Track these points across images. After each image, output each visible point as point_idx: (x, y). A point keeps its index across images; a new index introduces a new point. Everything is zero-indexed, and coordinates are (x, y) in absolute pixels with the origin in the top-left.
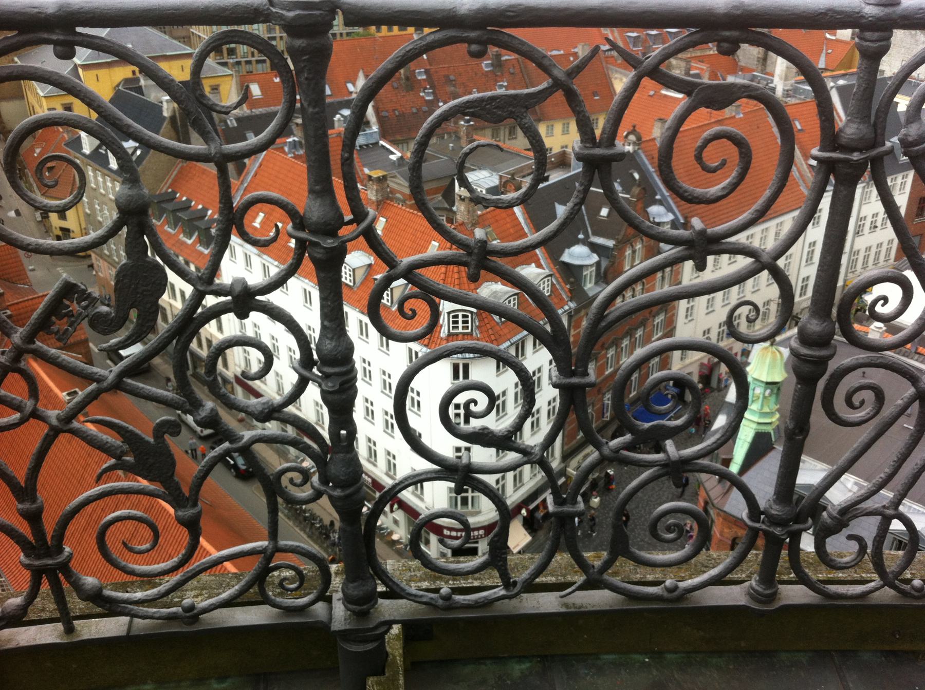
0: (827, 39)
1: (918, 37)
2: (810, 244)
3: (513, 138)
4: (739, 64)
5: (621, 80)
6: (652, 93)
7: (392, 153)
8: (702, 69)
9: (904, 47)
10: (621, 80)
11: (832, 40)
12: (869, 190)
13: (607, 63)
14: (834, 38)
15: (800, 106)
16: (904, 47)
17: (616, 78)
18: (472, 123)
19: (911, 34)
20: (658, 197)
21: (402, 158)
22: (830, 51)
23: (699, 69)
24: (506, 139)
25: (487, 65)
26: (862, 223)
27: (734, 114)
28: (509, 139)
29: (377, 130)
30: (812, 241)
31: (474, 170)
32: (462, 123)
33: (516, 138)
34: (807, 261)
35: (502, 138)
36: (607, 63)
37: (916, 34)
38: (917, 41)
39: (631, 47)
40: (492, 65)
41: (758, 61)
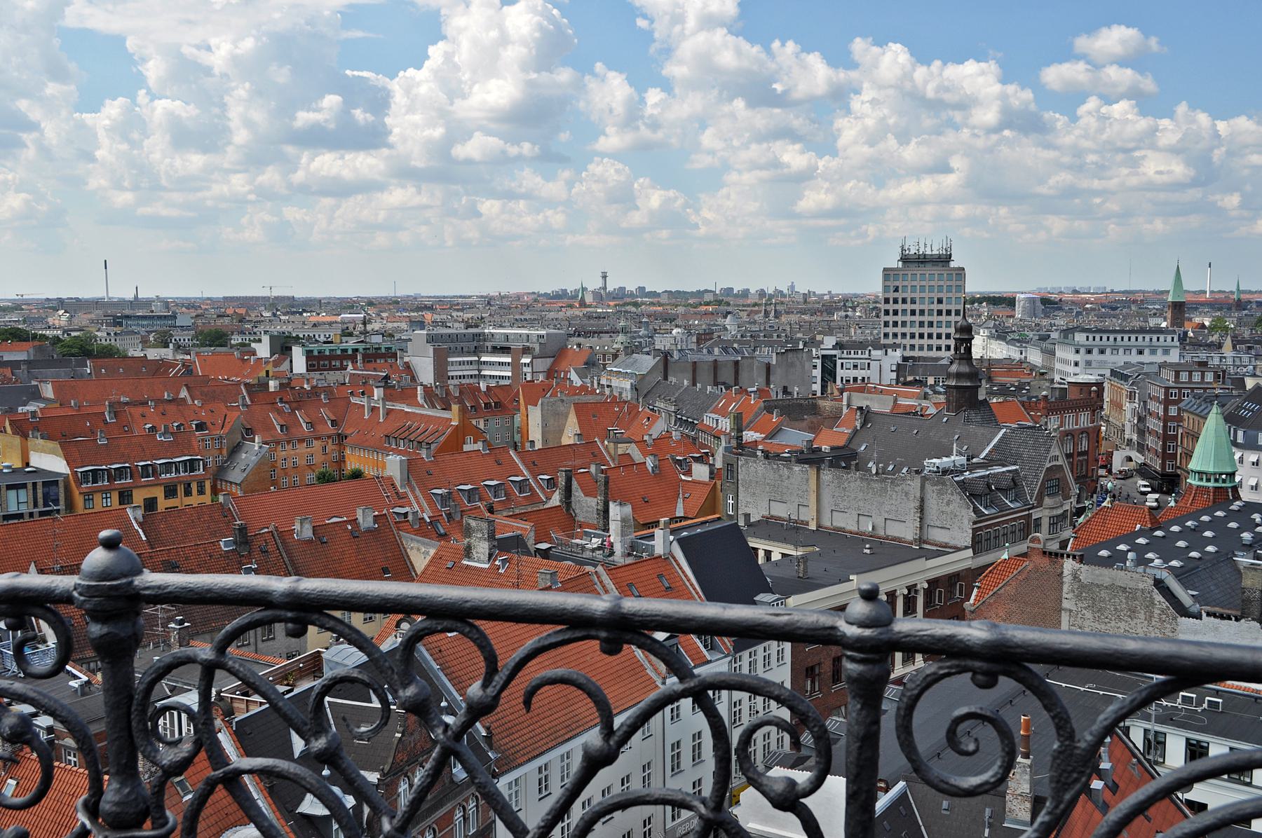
0: (682, 480)
1: (781, 472)
2: (673, 745)
3: (268, 639)
4: (576, 518)
5: (418, 550)
6: (450, 565)
7: (75, 677)
8: (526, 529)
9: (768, 484)
10: (418, 550)
11: (689, 481)
12: (737, 665)
13: (399, 529)
14: (690, 479)
15: (635, 566)
16: (768, 484)
17: (412, 548)
18: (186, 624)
19: (773, 469)
20: (444, 704)
21: (88, 683)
22: (686, 495)
23: (522, 529)
24: (259, 642)
25: (226, 544)
26: (737, 709)
27: (549, 584)
28: (263, 641)
29: (54, 646)
30: (675, 740)
31: (191, 690)
32: (173, 625)
33: (273, 639)
34: (673, 770)
35: (252, 640)
36: (399, 529)
37: (778, 469)
38: (781, 476)
39: (439, 507)
40: (235, 542)
41: (598, 514)
